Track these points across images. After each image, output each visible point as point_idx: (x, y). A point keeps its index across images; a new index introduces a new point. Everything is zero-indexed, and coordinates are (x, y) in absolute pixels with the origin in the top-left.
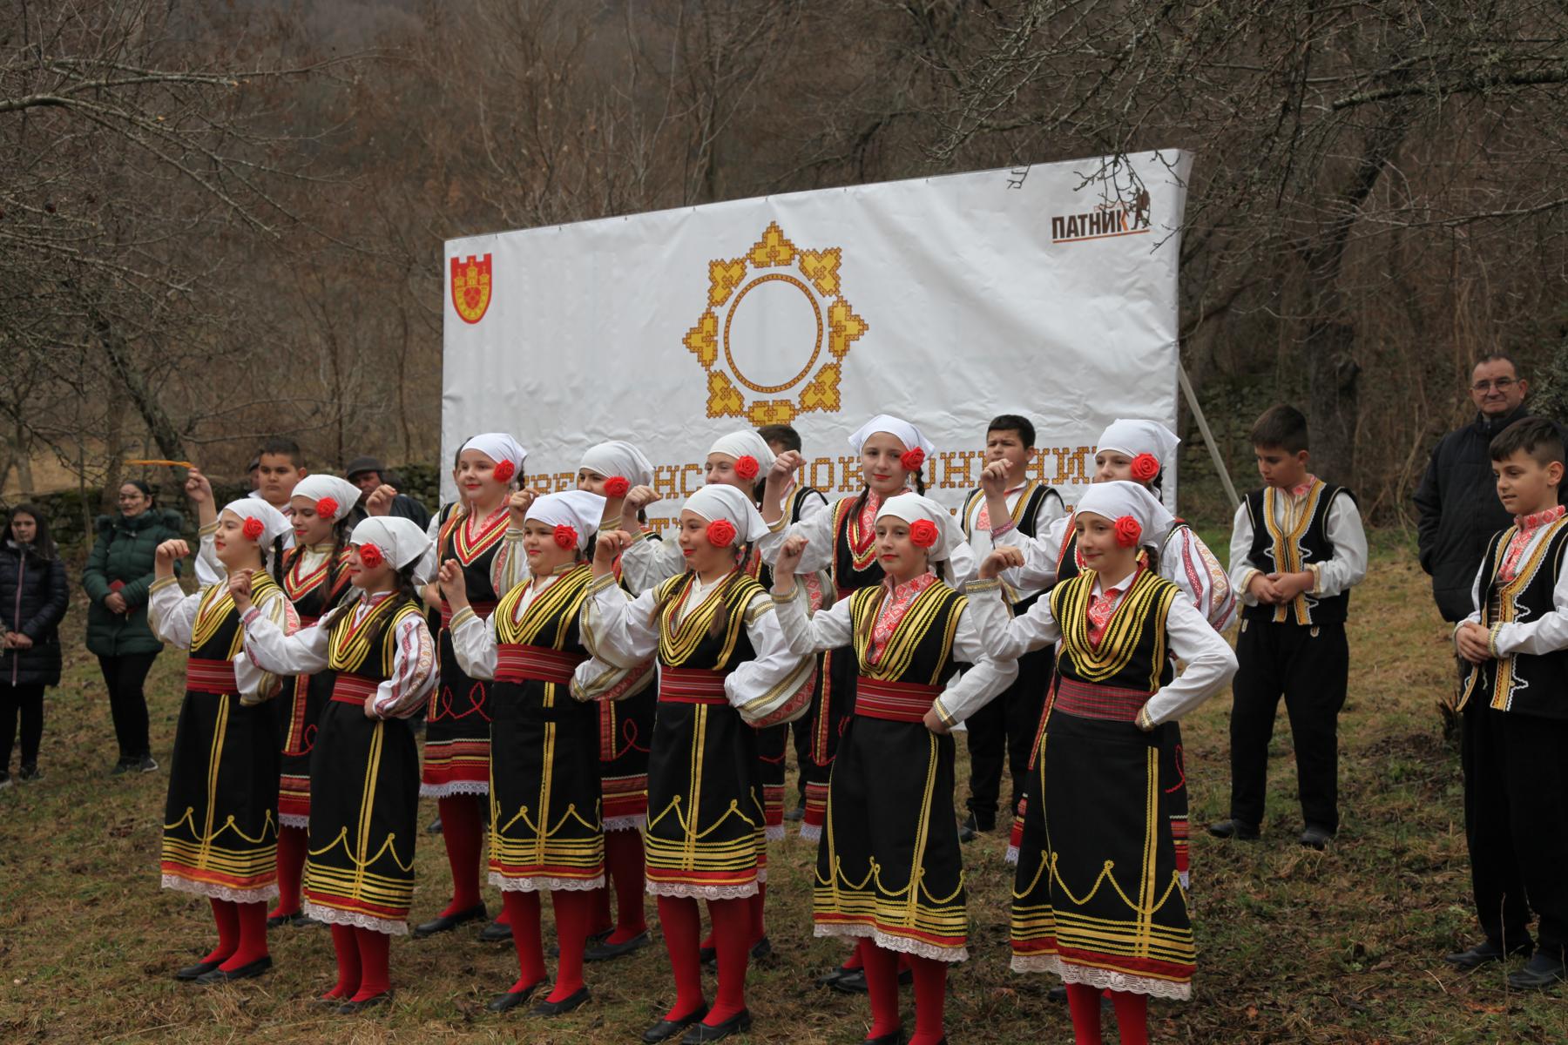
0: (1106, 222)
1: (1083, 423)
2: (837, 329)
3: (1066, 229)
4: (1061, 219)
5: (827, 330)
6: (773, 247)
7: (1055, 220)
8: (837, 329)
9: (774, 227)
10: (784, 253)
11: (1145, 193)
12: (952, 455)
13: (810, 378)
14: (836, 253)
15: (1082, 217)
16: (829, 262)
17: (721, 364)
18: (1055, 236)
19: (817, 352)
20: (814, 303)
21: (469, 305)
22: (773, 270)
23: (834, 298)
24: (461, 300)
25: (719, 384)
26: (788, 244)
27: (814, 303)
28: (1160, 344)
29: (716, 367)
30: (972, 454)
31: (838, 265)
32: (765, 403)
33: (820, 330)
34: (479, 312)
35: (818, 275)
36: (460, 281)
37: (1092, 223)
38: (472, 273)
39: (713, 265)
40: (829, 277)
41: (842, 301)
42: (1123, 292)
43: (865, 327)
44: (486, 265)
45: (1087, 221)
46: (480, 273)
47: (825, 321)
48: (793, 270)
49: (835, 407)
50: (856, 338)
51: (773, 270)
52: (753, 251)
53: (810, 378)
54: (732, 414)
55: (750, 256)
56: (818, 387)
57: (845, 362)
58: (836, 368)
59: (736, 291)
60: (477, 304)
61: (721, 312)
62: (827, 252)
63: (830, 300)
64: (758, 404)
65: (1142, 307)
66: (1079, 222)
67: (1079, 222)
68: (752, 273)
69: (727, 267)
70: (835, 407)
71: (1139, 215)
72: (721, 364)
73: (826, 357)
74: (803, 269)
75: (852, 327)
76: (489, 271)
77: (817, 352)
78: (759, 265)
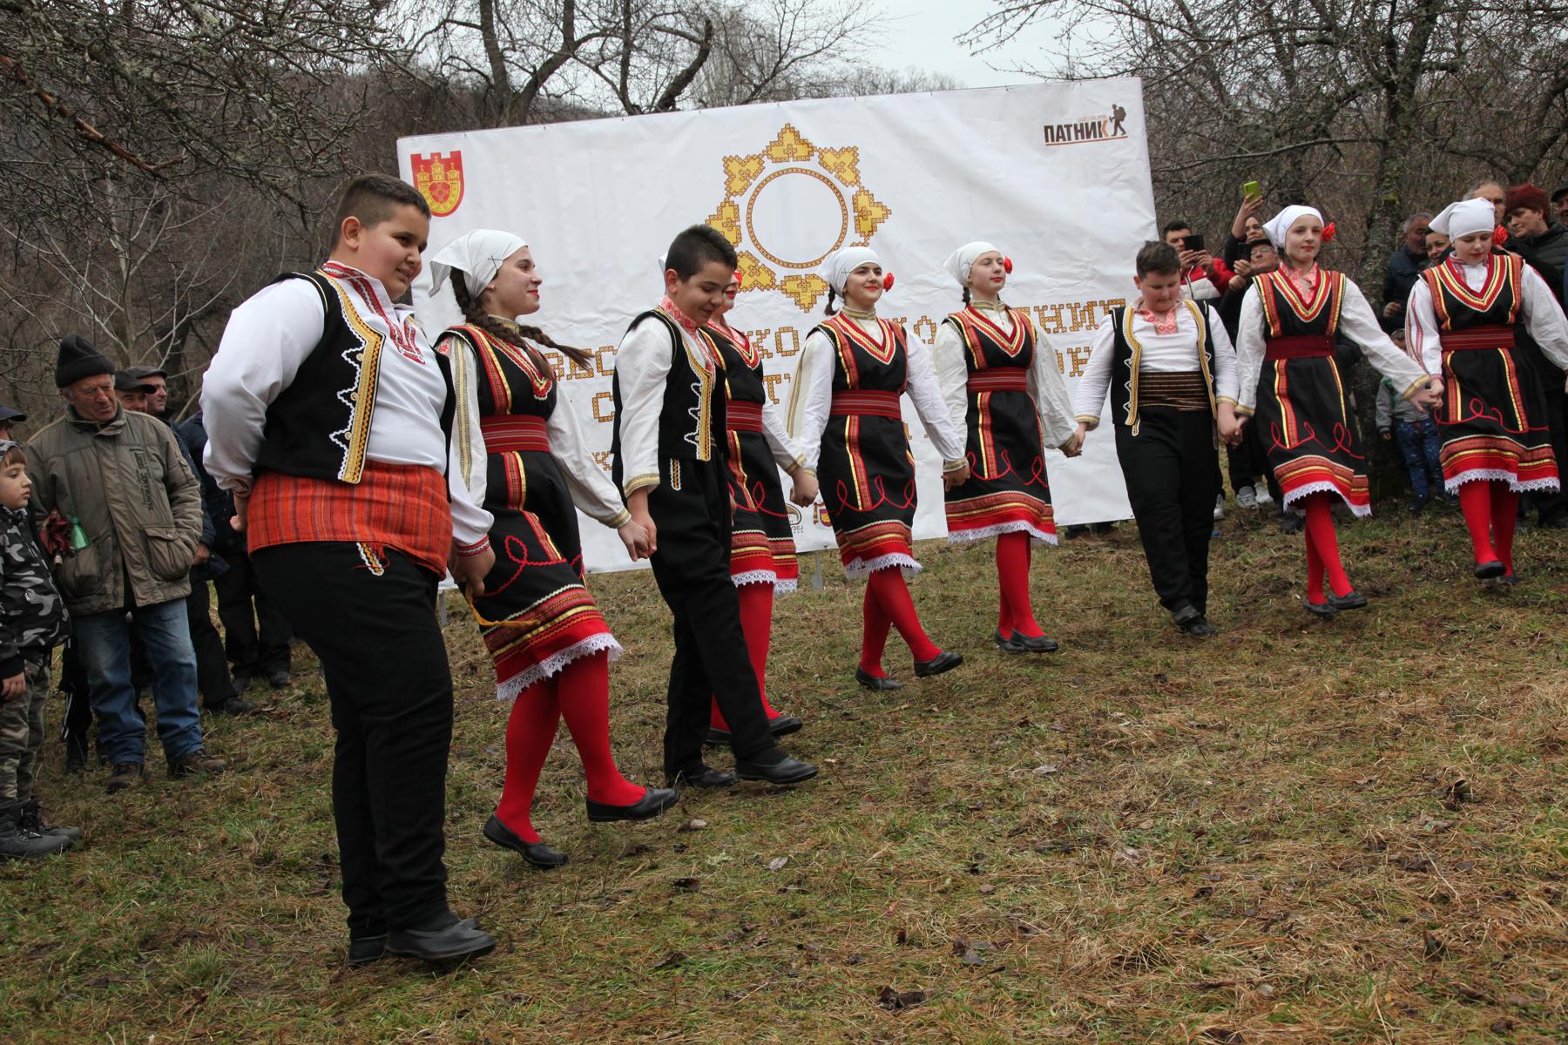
0: (1089, 131)
1: (1090, 283)
3: (1055, 135)
5: (851, 215)
6: (791, 145)
8: (862, 215)
9: (789, 128)
10: (802, 151)
12: (1045, 307)
15: (1068, 127)
20: (837, 192)
21: (436, 198)
22: (792, 164)
26: (805, 142)
27: (837, 192)
28: (1146, 222)
30: (1061, 306)
31: (856, 161)
32: (798, 277)
33: (845, 215)
34: (449, 206)
37: (1076, 131)
38: (438, 171)
39: (727, 161)
40: (849, 171)
41: (862, 190)
42: (1109, 183)
43: (887, 212)
44: (455, 161)
46: (448, 168)
47: (850, 207)
51: (792, 164)
52: (769, 148)
54: (763, 288)
55: (767, 152)
59: (755, 184)
60: (446, 198)
61: (742, 202)
62: (844, 150)
63: (853, 190)
64: (790, 278)
65: (1126, 194)
68: (770, 167)
69: (743, 163)
71: (1117, 125)
74: (823, 164)
75: (877, 212)
76: (459, 167)
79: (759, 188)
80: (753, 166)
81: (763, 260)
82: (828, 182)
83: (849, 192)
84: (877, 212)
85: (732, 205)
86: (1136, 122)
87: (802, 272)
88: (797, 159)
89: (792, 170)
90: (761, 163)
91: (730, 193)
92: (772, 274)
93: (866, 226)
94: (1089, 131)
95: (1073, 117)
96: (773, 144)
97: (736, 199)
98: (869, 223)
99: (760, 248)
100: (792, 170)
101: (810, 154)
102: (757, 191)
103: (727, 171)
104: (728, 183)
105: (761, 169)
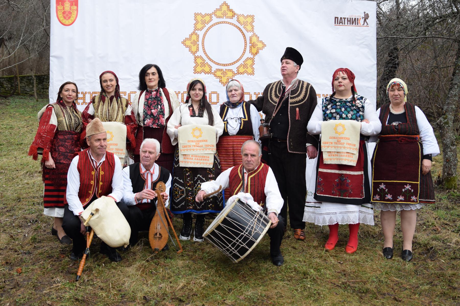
0: (353, 21)
2: (253, 45)
3: (339, 21)
4: (338, 18)
5: (248, 45)
7: (335, 18)
8: (253, 45)
10: (230, 14)
11: (367, 14)
13: (241, 62)
14: (252, 17)
15: (345, 18)
16: (249, 20)
17: (200, 53)
18: (335, 23)
19: (244, 53)
20: (243, 34)
21: (65, 18)
22: (224, 20)
23: (252, 33)
24: (61, 15)
25: (199, 61)
26: (231, 11)
27: (243, 34)
29: (198, 54)
32: (221, 70)
33: (246, 44)
34: (70, 21)
35: (245, 24)
36: (60, 7)
39: (196, 15)
40: (249, 25)
41: (255, 35)
43: (264, 45)
45: (346, 20)
46: (72, 5)
48: (234, 21)
49: (253, 73)
50: (261, 49)
51: (224, 20)
53: (241, 62)
55: (214, 13)
56: (245, 66)
57: (256, 57)
58: (253, 59)
60: (69, 18)
62: (248, 16)
64: (218, 70)
66: (343, 20)
67: (343, 20)
68: (215, 20)
69: (203, 16)
70: (253, 73)
71: (365, 20)
72: (200, 53)
73: (248, 54)
74: (238, 21)
75: (260, 45)
77: (244, 53)
78: (219, 17)
79: (209, 28)
80: (207, 18)
81: (207, 60)
82: (240, 29)
83: (248, 35)
84: (260, 45)
85: (196, 34)
86: (373, 21)
87: (224, 68)
88: (227, 18)
89: (224, 22)
90: (211, 18)
91: (196, 29)
92: (210, 67)
93: (254, 50)
94: (353, 21)
95: (347, 15)
96: (217, 10)
97: (198, 32)
98: (256, 49)
99: (207, 55)
100: (224, 22)
101: (233, 16)
102: (208, 30)
103: (196, 19)
104: (195, 24)
105: (211, 20)
